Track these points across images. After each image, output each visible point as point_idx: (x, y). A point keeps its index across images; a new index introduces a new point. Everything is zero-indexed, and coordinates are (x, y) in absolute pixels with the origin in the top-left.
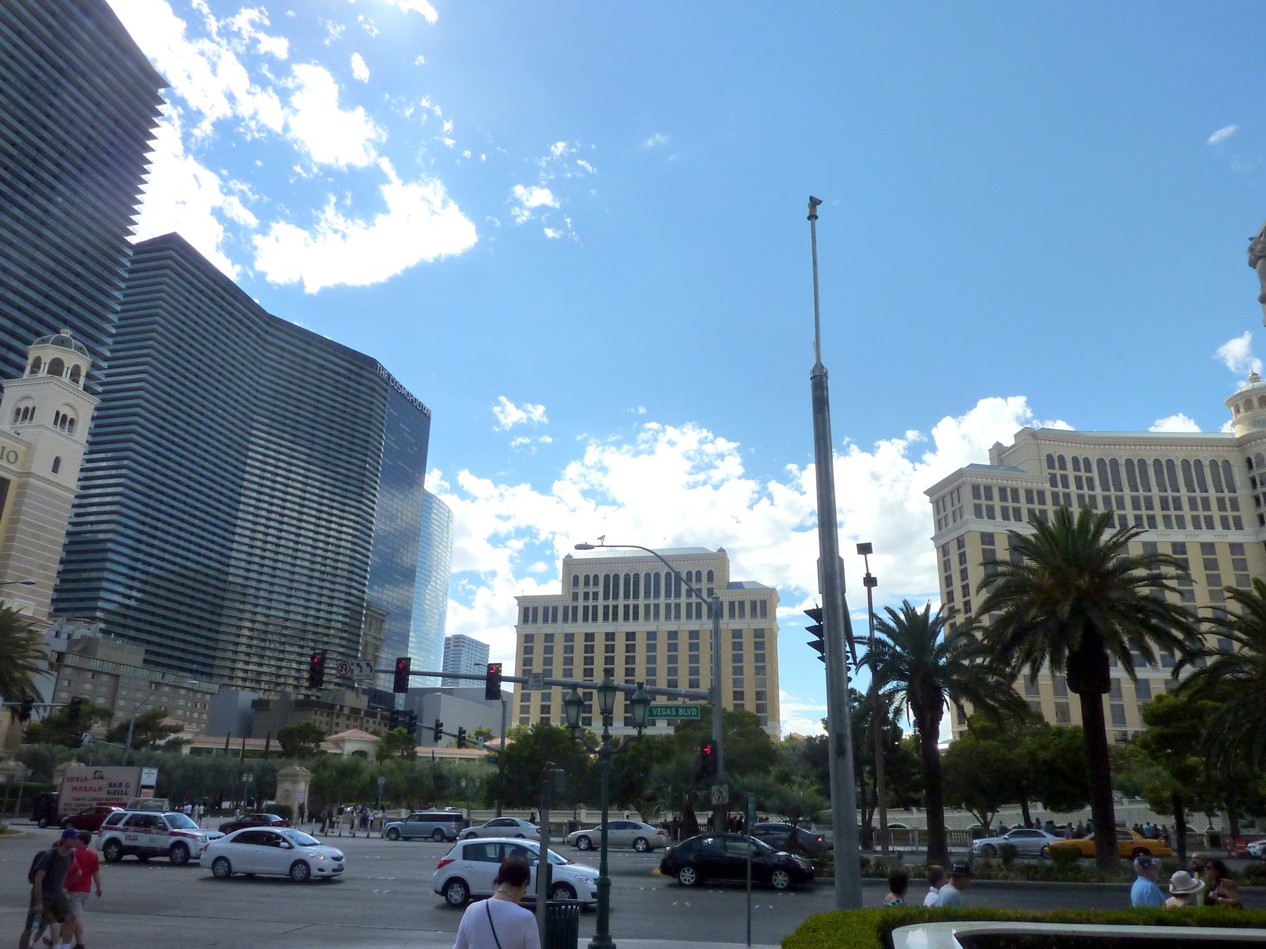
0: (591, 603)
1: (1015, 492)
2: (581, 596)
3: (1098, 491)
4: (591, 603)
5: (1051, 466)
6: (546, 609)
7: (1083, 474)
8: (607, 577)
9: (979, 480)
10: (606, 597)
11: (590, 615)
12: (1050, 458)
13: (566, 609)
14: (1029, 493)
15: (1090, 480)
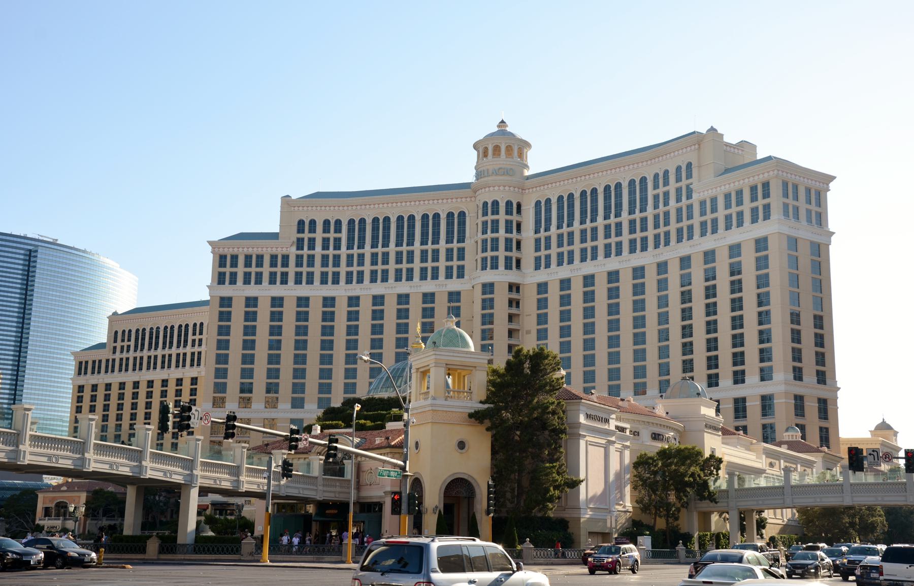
0: (125, 355)
1: (260, 258)
2: (118, 349)
3: (344, 251)
4: (125, 355)
5: (300, 229)
6: (94, 362)
7: (332, 235)
8: (137, 331)
9: (226, 250)
10: (135, 351)
11: (124, 366)
12: (301, 223)
13: (108, 361)
14: (274, 258)
15: (338, 241)
